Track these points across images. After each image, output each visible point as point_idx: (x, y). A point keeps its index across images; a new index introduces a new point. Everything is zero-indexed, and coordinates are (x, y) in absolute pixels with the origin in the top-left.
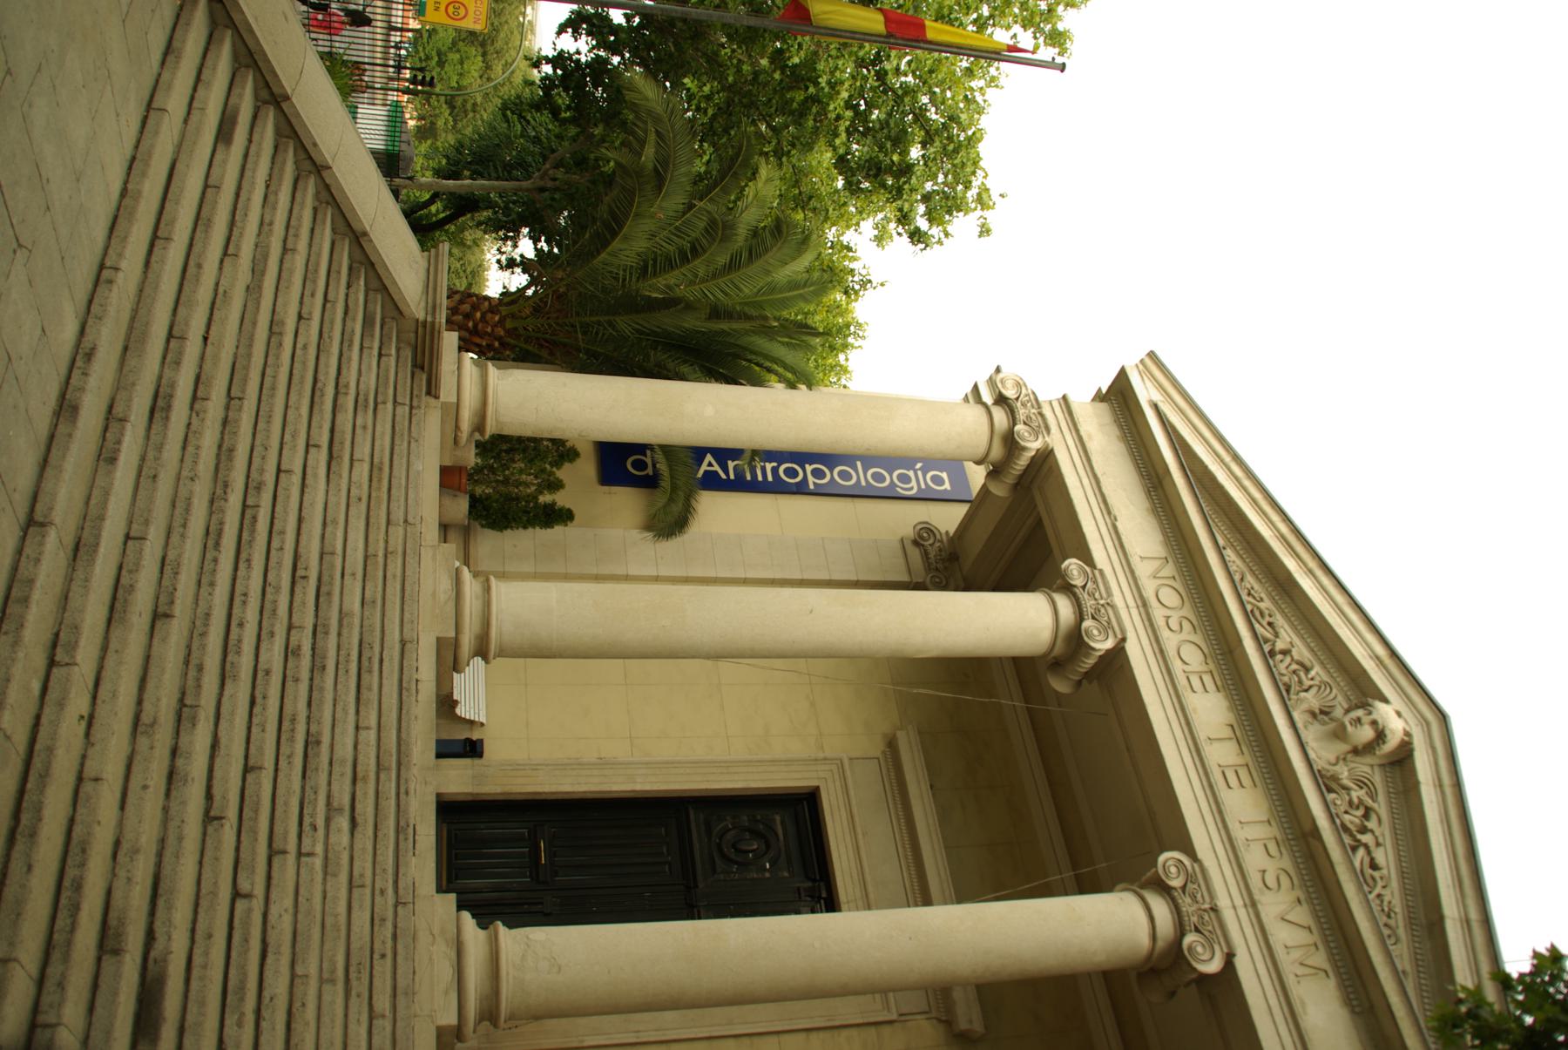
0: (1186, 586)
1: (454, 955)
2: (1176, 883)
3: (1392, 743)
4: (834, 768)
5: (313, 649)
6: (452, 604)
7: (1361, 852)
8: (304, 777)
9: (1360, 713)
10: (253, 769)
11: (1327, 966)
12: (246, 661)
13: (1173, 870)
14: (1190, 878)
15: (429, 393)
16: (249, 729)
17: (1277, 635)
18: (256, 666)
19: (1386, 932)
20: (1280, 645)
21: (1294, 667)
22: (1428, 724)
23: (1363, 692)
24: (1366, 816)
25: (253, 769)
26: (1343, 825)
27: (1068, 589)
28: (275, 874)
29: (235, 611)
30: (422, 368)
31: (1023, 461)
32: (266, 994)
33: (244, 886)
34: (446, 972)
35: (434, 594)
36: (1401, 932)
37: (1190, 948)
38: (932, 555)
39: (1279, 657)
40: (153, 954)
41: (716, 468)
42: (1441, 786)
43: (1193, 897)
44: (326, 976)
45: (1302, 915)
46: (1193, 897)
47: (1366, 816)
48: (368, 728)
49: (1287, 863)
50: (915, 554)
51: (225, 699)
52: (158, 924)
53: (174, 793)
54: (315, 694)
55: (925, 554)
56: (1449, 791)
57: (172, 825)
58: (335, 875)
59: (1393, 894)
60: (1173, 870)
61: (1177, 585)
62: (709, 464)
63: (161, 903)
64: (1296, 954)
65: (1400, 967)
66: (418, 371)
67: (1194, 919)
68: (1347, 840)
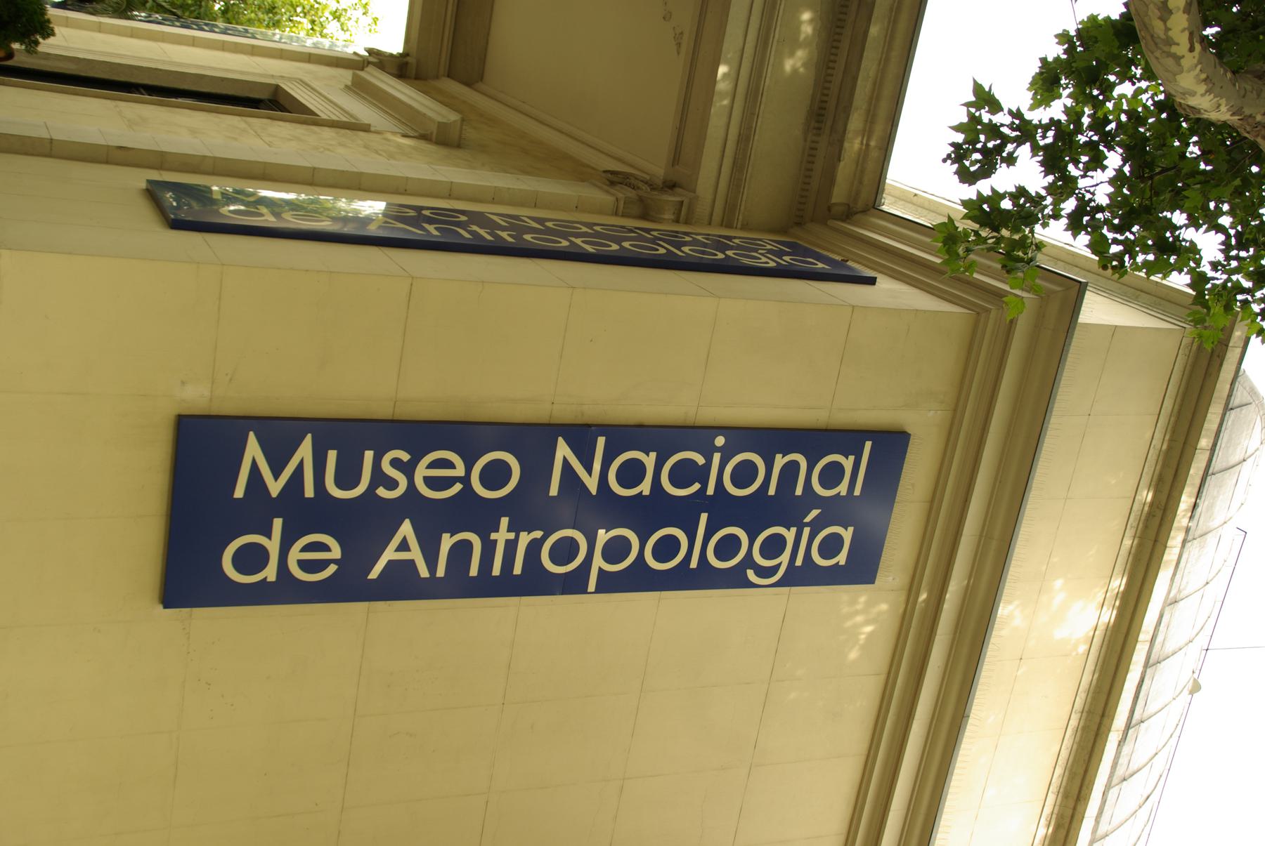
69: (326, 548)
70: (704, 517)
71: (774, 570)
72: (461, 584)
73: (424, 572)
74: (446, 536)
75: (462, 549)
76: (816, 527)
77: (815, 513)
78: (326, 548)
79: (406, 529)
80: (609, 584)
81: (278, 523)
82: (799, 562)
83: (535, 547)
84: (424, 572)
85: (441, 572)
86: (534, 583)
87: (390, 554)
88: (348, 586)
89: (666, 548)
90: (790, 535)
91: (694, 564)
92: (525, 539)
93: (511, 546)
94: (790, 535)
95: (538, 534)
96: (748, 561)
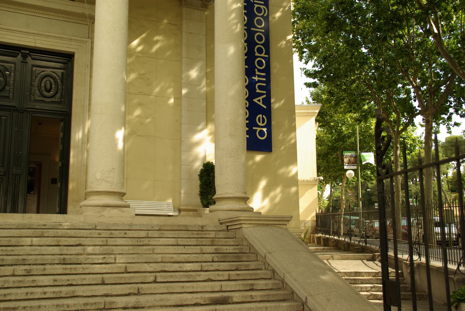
1: (109, 208)
5: (12, 265)
8: (80, 264)
10: (103, 281)
12: (64, 289)
16: (83, 285)
18: (51, 286)
25: (103, 281)
28: (135, 270)
29: (37, 297)
32: (178, 270)
33: (152, 279)
34: (115, 212)
40: (202, 303)
41: (261, 98)
44: (151, 252)
48: (32, 241)
51: (85, 295)
52: (192, 303)
53: (143, 305)
54: (38, 263)
57: (156, 304)
58: (113, 250)
62: (258, 101)
63: (184, 303)
69: (259, 118)
70: (252, 29)
71: (264, 8)
72: (267, 89)
73: (265, 96)
74: (257, 91)
75: (260, 87)
78: (259, 118)
79: (255, 100)
80: (268, 52)
81: (254, 128)
83: (259, 71)
84: (265, 96)
85: (265, 92)
86: (267, 70)
87: (261, 104)
88: (268, 112)
90: (256, 6)
91: (263, 31)
92: (257, 73)
93: (259, 76)
94: (256, 6)
95: (256, 70)
96: (262, 17)
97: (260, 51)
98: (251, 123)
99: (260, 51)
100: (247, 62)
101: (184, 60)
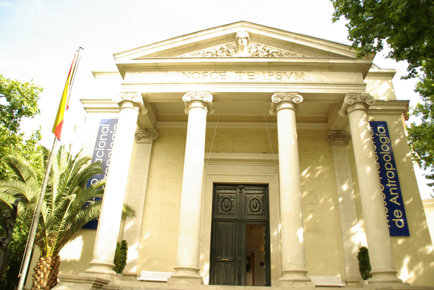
0: (194, 70)
1: (297, 282)
2: (280, 100)
3: (248, 36)
4: (208, 177)
6: (190, 280)
7: (274, 54)
9: (240, 41)
11: (301, 72)
13: (277, 99)
14: (278, 96)
15: (107, 284)
17: (211, 52)
19: (293, 56)
20: (214, 52)
21: (221, 51)
22: (243, 25)
23: (233, 37)
24: (265, 50)
26: (266, 55)
27: (191, 102)
30: (102, 285)
31: (142, 103)
34: (301, 284)
35: (186, 285)
36: (294, 53)
37: (297, 102)
38: (144, 135)
39: (217, 54)
41: (395, 198)
42: (260, 29)
43: (284, 97)
45: (288, 73)
46: (284, 97)
47: (265, 50)
49: (275, 72)
50: (143, 140)
55: (144, 137)
56: (262, 28)
59: (284, 51)
60: (277, 99)
61: (192, 72)
62: (394, 200)
64: (298, 78)
65: (301, 57)
66: (102, 287)
67: (289, 98)
68: (270, 56)
70: (381, 153)
72: (398, 191)
75: (393, 191)
76: (378, 133)
77: (377, 134)
79: (391, 200)
80: (394, 166)
81: (393, 220)
82: (385, 135)
83: (391, 180)
84: (397, 197)
86: (396, 178)
87: (395, 202)
88: (402, 208)
89: (387, 158)
90: (381, 138)
91: (389, 153)
92: (389, 181)
93: (391, 183)
95: (388, 179)
96: (386, 144)
97: (389, 166)
98: (390, 216)
99: (389, 166)
100: (380, 175)
101: (337, 179)
